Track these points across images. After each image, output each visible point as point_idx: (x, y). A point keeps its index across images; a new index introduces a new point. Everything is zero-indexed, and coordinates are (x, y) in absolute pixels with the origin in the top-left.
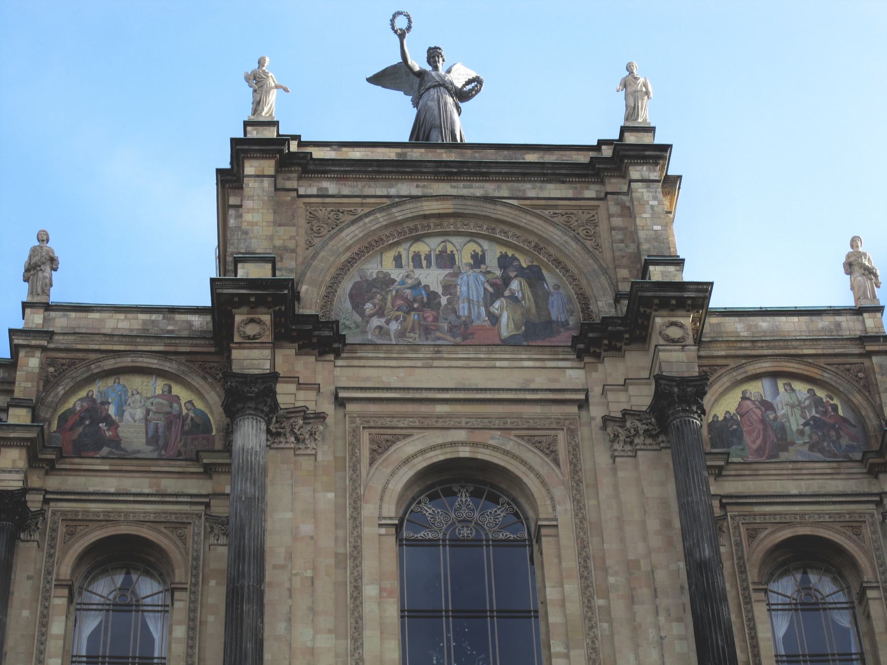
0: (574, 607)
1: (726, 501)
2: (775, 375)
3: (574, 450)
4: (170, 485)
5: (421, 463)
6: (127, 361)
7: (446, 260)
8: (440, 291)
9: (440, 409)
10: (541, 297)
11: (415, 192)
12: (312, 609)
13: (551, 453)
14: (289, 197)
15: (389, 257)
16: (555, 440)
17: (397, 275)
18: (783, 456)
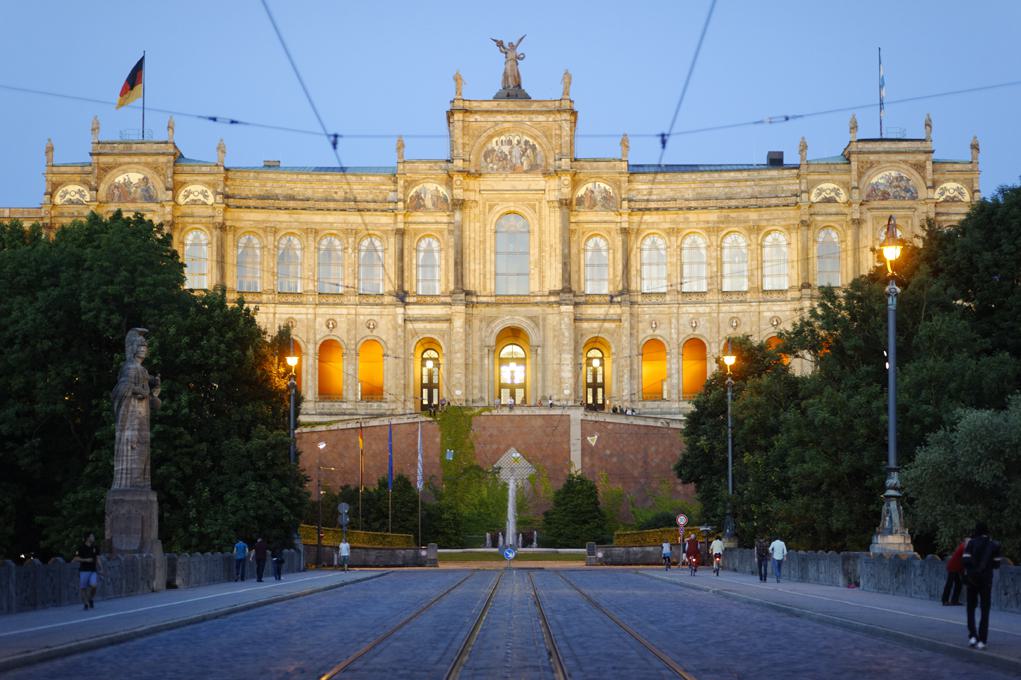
0: (537, 256)
3: (540, 208)
5: (501, 212)
8: (507, 153)
9: (507, 196)
10: (535, 156)
11: (502, 119)
12: (475, 259)
13: (533, 207)
14: (466, 124)
15: (494, 140)
16: (535, 205)
17: (496, 148)
18: (595, 209)
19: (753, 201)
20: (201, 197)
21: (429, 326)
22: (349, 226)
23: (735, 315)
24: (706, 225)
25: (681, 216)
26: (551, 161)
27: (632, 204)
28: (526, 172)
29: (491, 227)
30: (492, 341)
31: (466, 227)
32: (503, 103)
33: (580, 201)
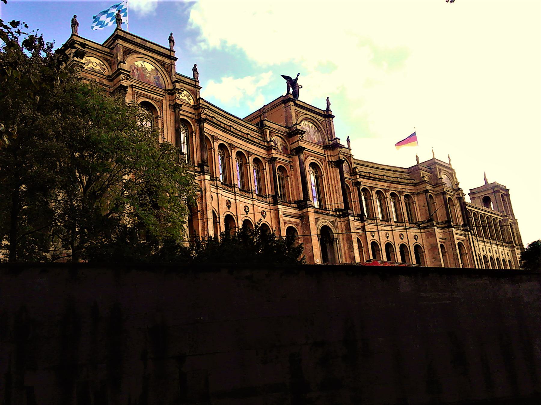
6: (278, 134)
7: (309, 126)
9: (312, 153)
11: (306, 113)
13: (322, 164)
15: (303, 122)
17: (304, 127)
20: (186, 98)
21: (292, 219)
23: (401, 233)
24: (384, 188)
25: (374, 182)
26: (327, 140)
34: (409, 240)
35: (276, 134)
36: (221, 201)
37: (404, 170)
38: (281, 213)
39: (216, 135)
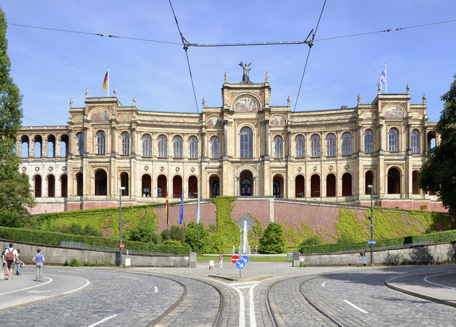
0: (255, 143)
1: (271, 131)
2: (277, 115)
4: (219, 129)
5: (242, 127)
6: (213, 115)
7: (245, 100)
14: (229, 93)
17: (240, 102)
19: (339, 121)
22: (184, 132)
23: (331, 165)
24: (320, 131)
26: (261, 107)
27: (292, 123)
28: (251, 112)
29: (238, 132)
30: (238, 176)
31: (228, 132)
32: (243, 85)
33: (272, 122)
34: (338, 170)
35: (212, 115)
36: (155, 168)
37: (351, 111)
38: (203, 167)
39: (155, 131)
